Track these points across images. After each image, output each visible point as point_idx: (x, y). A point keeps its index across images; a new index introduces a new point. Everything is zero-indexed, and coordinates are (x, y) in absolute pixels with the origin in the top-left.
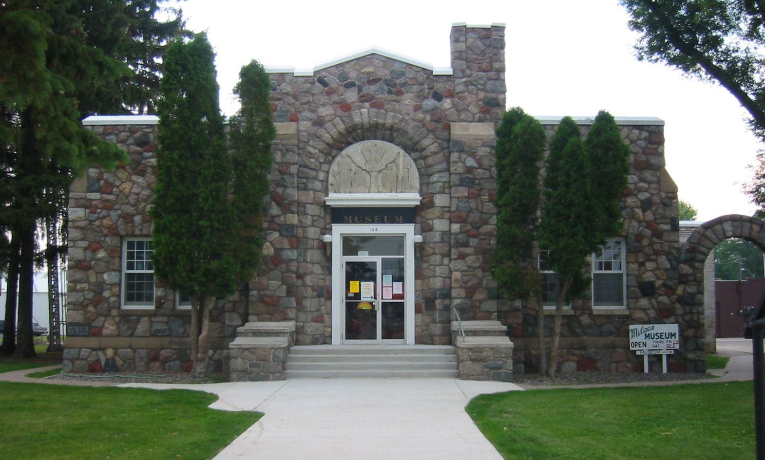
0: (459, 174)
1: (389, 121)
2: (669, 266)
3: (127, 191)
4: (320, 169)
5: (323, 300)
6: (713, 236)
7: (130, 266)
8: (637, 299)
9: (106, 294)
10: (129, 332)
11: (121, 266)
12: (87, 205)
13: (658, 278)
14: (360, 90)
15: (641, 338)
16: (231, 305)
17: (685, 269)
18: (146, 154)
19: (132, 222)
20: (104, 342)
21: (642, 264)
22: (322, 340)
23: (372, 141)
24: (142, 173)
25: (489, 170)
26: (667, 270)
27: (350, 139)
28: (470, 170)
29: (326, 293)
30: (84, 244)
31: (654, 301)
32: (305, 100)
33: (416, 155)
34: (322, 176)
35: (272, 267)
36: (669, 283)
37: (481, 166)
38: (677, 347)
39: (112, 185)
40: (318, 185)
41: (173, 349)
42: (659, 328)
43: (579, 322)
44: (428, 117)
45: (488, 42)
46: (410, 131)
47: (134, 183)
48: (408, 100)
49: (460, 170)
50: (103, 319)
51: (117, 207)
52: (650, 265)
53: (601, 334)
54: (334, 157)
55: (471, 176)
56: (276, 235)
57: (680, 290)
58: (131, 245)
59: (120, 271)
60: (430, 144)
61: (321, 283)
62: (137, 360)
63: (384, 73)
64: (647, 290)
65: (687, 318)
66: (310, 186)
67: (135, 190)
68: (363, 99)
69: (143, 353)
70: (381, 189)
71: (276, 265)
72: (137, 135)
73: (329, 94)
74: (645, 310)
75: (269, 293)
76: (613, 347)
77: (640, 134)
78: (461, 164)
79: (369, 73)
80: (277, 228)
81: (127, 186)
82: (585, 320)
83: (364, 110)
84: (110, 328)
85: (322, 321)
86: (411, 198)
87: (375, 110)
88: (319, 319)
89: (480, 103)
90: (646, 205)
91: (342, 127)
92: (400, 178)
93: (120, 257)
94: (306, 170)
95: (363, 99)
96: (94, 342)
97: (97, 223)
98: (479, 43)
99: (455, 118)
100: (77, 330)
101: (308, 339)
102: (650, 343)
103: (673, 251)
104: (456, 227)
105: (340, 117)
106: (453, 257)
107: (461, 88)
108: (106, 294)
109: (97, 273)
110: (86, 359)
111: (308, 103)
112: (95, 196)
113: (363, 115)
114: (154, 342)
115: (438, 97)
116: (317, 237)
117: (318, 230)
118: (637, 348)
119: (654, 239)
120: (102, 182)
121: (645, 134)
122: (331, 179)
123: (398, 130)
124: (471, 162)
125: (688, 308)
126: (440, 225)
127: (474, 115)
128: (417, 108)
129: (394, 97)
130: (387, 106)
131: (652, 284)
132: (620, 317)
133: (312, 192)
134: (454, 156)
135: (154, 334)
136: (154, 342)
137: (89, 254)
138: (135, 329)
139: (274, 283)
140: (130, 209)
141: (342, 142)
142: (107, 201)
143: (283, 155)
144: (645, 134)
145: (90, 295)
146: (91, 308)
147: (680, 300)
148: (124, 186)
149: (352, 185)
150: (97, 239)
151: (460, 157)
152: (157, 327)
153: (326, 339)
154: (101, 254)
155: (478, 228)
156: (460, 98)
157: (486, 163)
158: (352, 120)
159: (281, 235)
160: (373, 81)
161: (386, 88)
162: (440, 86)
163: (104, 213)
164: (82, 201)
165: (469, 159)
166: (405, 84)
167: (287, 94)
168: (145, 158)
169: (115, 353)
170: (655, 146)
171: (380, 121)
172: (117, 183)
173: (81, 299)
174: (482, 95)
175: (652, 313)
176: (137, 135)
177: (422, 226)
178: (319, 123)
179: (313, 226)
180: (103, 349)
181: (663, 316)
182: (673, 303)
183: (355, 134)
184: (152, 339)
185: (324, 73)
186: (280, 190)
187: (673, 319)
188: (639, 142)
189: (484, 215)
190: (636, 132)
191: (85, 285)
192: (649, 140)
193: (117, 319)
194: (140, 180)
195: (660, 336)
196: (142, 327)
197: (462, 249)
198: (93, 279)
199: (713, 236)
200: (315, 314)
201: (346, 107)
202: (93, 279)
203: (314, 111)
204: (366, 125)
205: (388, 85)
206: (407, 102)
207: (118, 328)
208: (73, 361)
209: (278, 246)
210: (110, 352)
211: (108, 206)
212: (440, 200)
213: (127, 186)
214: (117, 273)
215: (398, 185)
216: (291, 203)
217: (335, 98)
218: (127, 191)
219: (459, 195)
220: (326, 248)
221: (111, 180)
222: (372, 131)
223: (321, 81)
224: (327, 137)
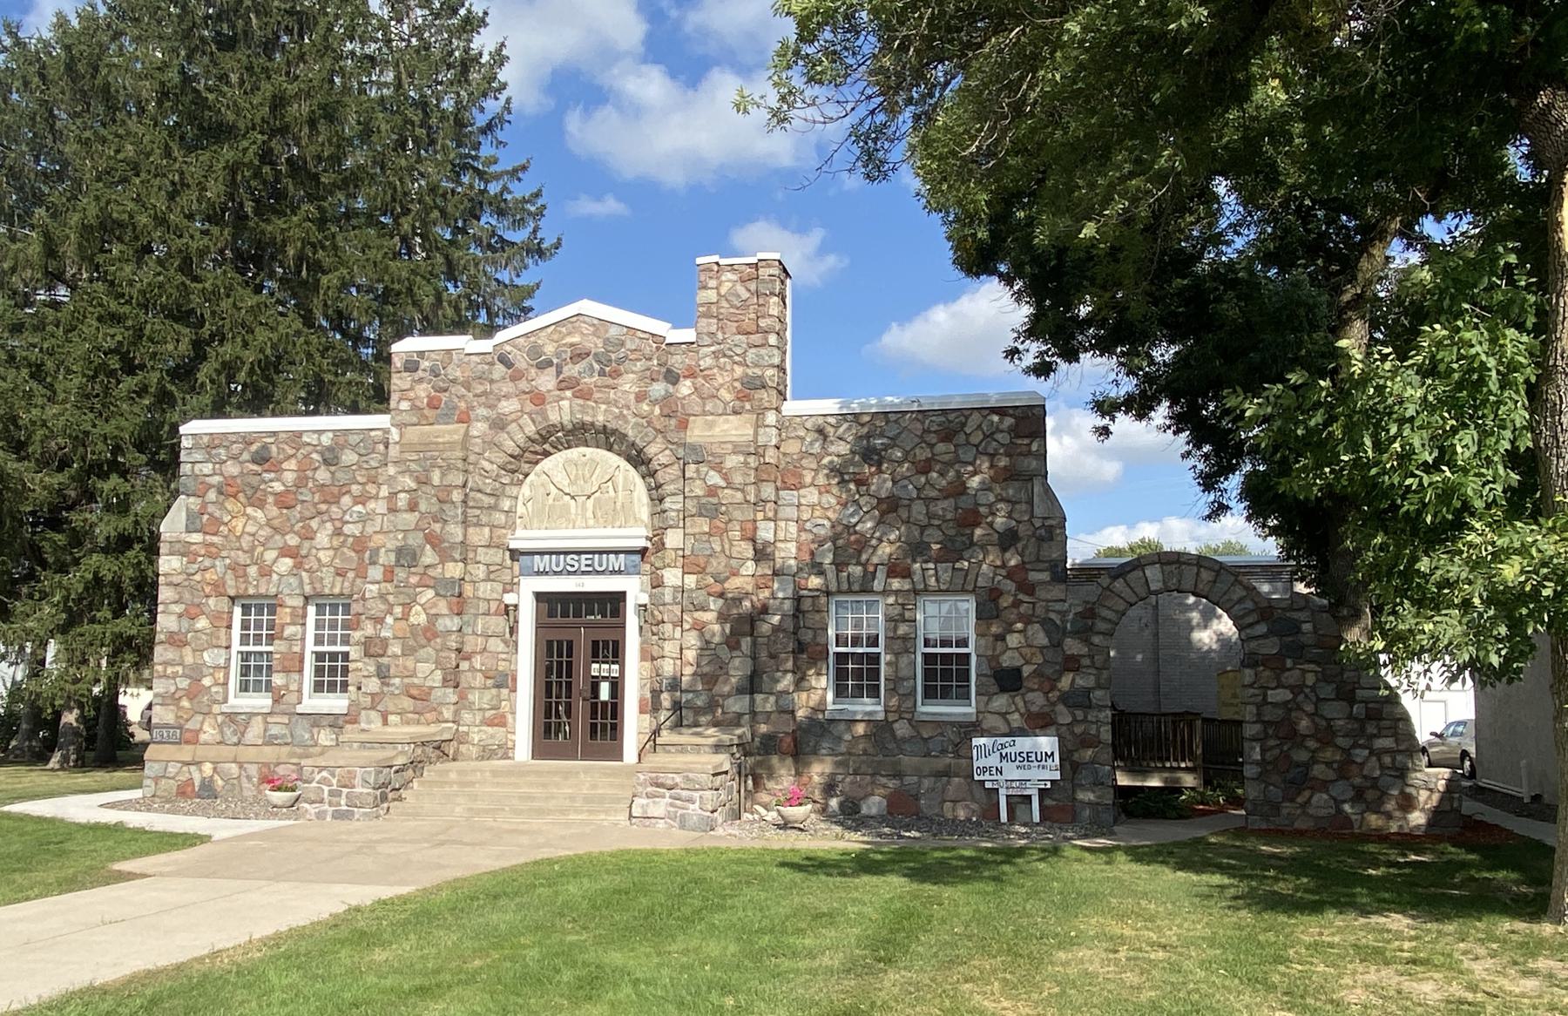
0: (697, 497)
1: (600, 419)
2: (1045, 642)
3: (239, 529)
4: (503, 493)
5: (505, 691)
6: (1127, 593)
7: (244, 640)
8: (991, 696)
9: (207, 682)
10: (235, 739)
11: (230, 639)
12: (185, 551)
13: (1027, 663)
14: (559, 373)
15: (993, 760)
16: (369, 699)
17: (1073, 646)
18: (267, 476)
19: (245, 575)
20: (201, 752)
21: (1001, 638)
22: (500, 753)
23: (582, 449)
24: (261, 505)
25: (743, 491)
26: (1042, 648)
27: (547, 446)
28: (712, 491)
29: (505, 681)
30: (178, 608)
31: (1018, 699)
32: (479, 389)
34: (506, 504)
35: (424, 642)
36: (1049, 671)
37: (729, 485)
38: (1057, 776)
39: (218, 522)
40: (500, 518)
42: (1024, 744)
43: (892, 732)
44: (657, 411)
45: (753, 286)
46: (630, 433)
47: (249, 517)
48: (628, 384)
49: (700, 493)
50: (199, 718)
51: (224, 554)
52: (1013, 640)
53: (928, 755)
54: (526, 475)
55: (715, 500)
56: (430, 593)
57: (1065, 682)
58: (246, 610)
59: (228, 647)
60: (656, 451)
61: (502, 666)
62: (244, 780)
63: (595, 345)
64: (1007, 680)
65: (1078, 730)
66: (484, 519)
67: (251, 529)
68: (565, 384)
69: (253, 770)
70: (591, 522)
71: (429, 640)
72: (254, 448)
73: (514, 379)
74: (1003, 715)
75: (416, 681)
76: (946, 773)
77: (1001, 421)
78: (698, 482)
79: (572, 345)
80: (432, 583)
81: (239, 524)
82: (902, 729)
83: (565, 403)
84: (209, 732)
85: (504, 725)
86: (637, 536)
87: (580, 401)
88: (500, 721)
89: (737, 384)
90: (1008, 540)
91: (531, 429)
92: (619, 504)
93: (229, 627)
94: (479, 495)
95: (565, 384)
96: (186, 752)
97: (197, 577)
98: (740, 289)
99: (698, 409)
101: (474, 751)
102: (1012, 772)
103: (1053, 616)
104: (691, 581)
105: (530, 414)
106: (686, 626)
107: (708, 362)
108: (207, 682)
111: (484, 393)
112: (196, 538)
113: (563, 411)
114: (269, 753)
115: (672, 378)
116: (495, 596)
117: (500, 587)
118: (987, 776)
119: (1021, 596)
120: (206, 517)
121: (1009, 421)
122: (520, 510)
123: (614, 432)
124: (715, 479)
125: (1079, 714)
126: (672, 577)
127: (726, 404)
128: (640, 397)
129: (610, 381)
130: (597, 395)
131: (1018, 670)
132: (960, 725)
133: (487, 530)
134: (691, 470)
135: (270, 741)
136: (269, 753)
137: (185, 623)
138: (243, 734)
139: (424, 668)
140: (243, 558)
141: (536, 453)
142: (212, 544)
143: (443, 475)
144: (1009, 421)
145: (184, 683)
146: (185, 703)
147: (1065, 698)
148: (234, 523)
149: (552, 515)
150: (196, 601)
151: (698, 471)
152: (274, 730)
153: (505, 751)
154: (202, 623)
155: (722, 582)
156: (704, 377)
157: (738, 479)
158: (546, 418)
159: (437, 594)
160: (579, 355)
161: (596, 366)
162: (677, 361)
163: (207, 563)
164: (178, 546)
165: (712, 473)
166: (620, 361)
167: (454, 381)
168: (264, 482)
169: (215, 769)
170: (1026, 441)
171: (588, 419)
172: (226, 519)
173: (173, 689)
174: (739, 371)
175: (1016, 720)
176: (254, 448)
178: (499, 424)
179: (488, 580)
180: (198, 763)
181: (1038, 723)
182: (1054, 704)
183: (548, 441)
184: (267, 749)
185: (508, 348)
186: (437, 527)
187: (1053, 729)
188: (999, 436)
189: (733, 562)
190: (996, 418)
191: (180, 669)
192: (1015, 432)
193: (220, 719)
194: (259, 514)
195: (1026, 758)
196: (255, 731)
197: (698, 615)
198: (189, 659)
199: (1127, 593)
200: (489, 714)
201: (539, 399)
202: (189, 659)
203: (492, 407)
204: (570, 427)
205: (599, 362)
206: (627, 387)
207: (222, 732)
208: (156, 779)
209: (433, 611)
210: (208, 768)
211: (213, 552)
212: (673, 539)
213: (239, 524)
214: (223, 651)
215: (615, 514)
216: (452, 547)
217: (523, 385)
218: (239, 529)
219: (697, 530)
220: (509, 611)
221: (217, 514)
222: (579, 434)
223: (504, 360)
224: (510, 446)
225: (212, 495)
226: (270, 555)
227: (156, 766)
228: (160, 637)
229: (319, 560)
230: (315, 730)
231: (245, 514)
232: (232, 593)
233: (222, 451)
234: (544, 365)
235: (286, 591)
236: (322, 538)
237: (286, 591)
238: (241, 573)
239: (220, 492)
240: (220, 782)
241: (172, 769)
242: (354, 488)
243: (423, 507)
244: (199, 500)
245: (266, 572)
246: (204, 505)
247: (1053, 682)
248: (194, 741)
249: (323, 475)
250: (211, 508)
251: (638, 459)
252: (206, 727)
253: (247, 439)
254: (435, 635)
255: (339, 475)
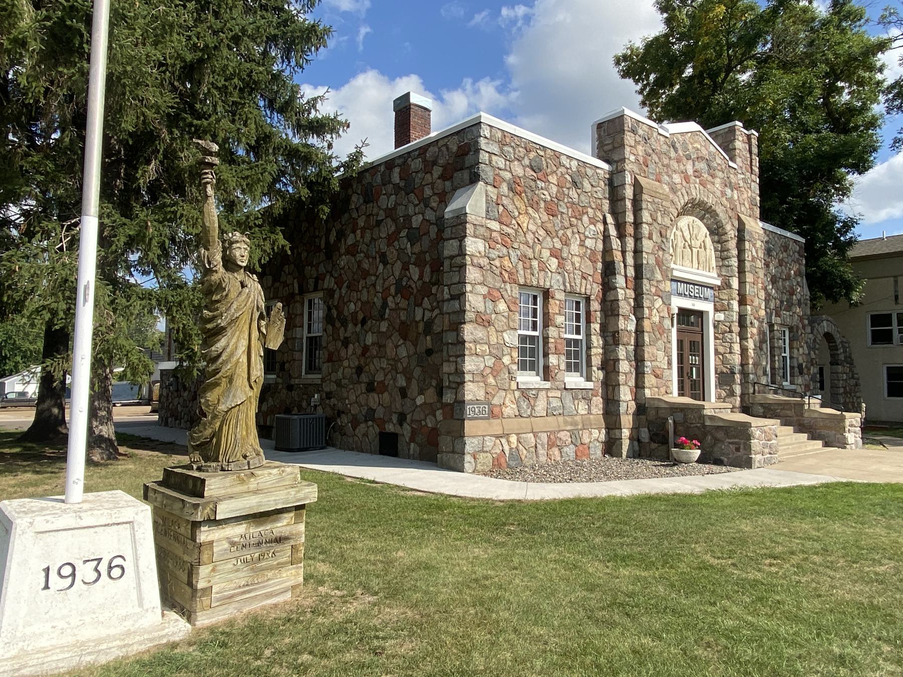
33: (716, 238)
41: (568, 431)
47: (531, 217)
69: (544, 437)
72: (532, 155)
73: (679, 161)
81: (524, 220)
96: (496, 426)
100: (477, 410)
109: (497, 331)
110: (489, 452)
112: (494, 225)
137: (490, 304)
140: (530, 253)
145: (490, 362)
146: (491, 380)
150: (498, 285)
163: (505, 250)
164: (482, 230)
169: (519, 441)
177: (715, 305)
184: (549, 419)
186: (661, 253)
198: (493, 340)
225: (504, 188)
226: (546, 253)
227: (475, 441)
228: (469, 315)
229: (573, 264)
230: (576, 402)
231: (527, 213)
232: (522, 281)
233: (511, 150)
234: (688, 158)
235: (556, 287)
236: (575, 248)
237: (556, 287)
238: (528, 265)
239: (511, 189)
240: (525, 452)
241: (489, 442)
242: (590, 210)
243: (654, 237)
244: (495, 190)
245: (543, 268)
246: (499, 196)
247: (809, 369)
248: (500, 416)
249: (573, 194)
250: (505, 201)
251: (716, 232)
252: (507, 402)
253: (529, 146)
254: (664, 332)
255: (583, 198)
